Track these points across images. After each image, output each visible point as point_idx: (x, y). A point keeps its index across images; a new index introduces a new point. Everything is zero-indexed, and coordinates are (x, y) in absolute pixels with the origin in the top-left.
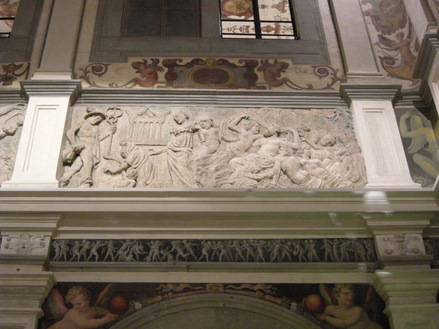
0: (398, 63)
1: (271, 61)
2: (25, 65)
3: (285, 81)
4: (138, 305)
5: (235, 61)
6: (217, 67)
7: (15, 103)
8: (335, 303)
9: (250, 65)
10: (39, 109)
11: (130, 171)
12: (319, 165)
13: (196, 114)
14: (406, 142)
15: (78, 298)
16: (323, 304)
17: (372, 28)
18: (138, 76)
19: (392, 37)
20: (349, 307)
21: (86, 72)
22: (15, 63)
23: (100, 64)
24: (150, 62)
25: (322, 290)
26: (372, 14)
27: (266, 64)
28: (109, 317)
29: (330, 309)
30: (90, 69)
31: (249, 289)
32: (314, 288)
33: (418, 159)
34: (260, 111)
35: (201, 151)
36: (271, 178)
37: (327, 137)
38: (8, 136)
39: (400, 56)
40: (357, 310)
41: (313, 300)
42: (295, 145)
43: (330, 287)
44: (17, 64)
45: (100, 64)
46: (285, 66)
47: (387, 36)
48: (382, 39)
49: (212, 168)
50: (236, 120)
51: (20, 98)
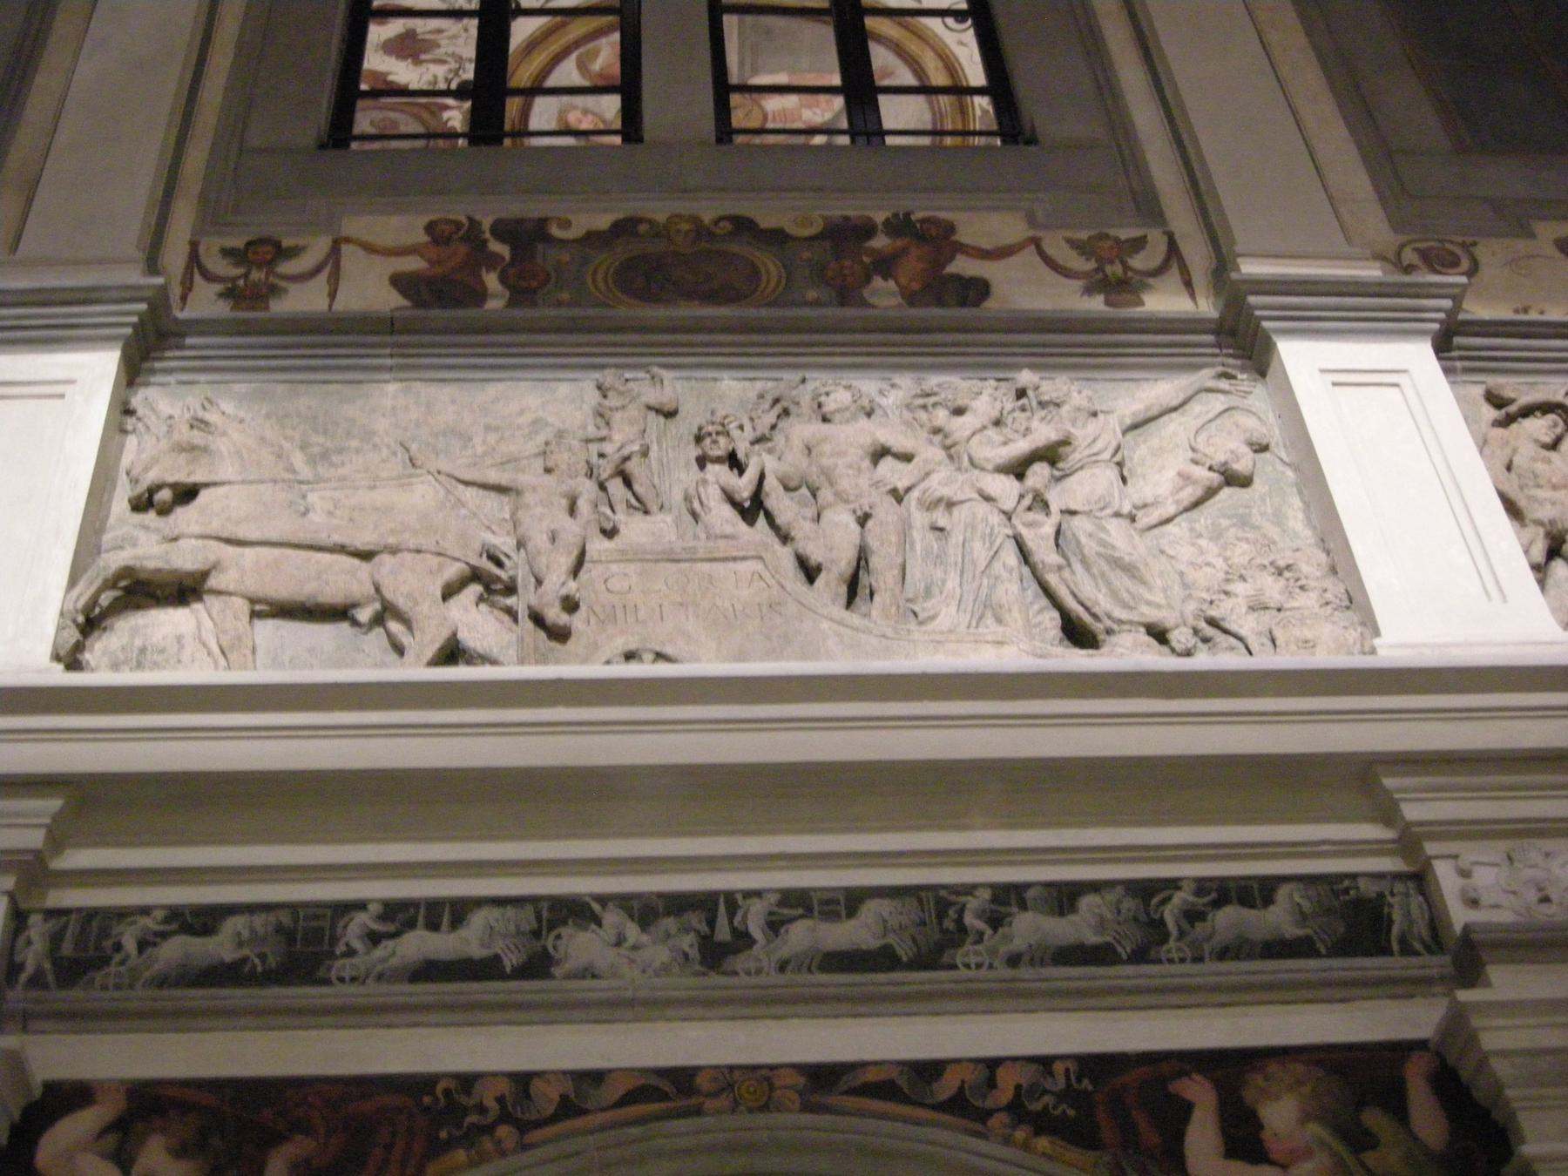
7: (1199, 367)
10: (1334, 384)
22: (1113, 232)
23: (1441, 241)
38: (1226, 492)
44: (1124, 234)
45: (1441, 241)
51: (1217, 351)
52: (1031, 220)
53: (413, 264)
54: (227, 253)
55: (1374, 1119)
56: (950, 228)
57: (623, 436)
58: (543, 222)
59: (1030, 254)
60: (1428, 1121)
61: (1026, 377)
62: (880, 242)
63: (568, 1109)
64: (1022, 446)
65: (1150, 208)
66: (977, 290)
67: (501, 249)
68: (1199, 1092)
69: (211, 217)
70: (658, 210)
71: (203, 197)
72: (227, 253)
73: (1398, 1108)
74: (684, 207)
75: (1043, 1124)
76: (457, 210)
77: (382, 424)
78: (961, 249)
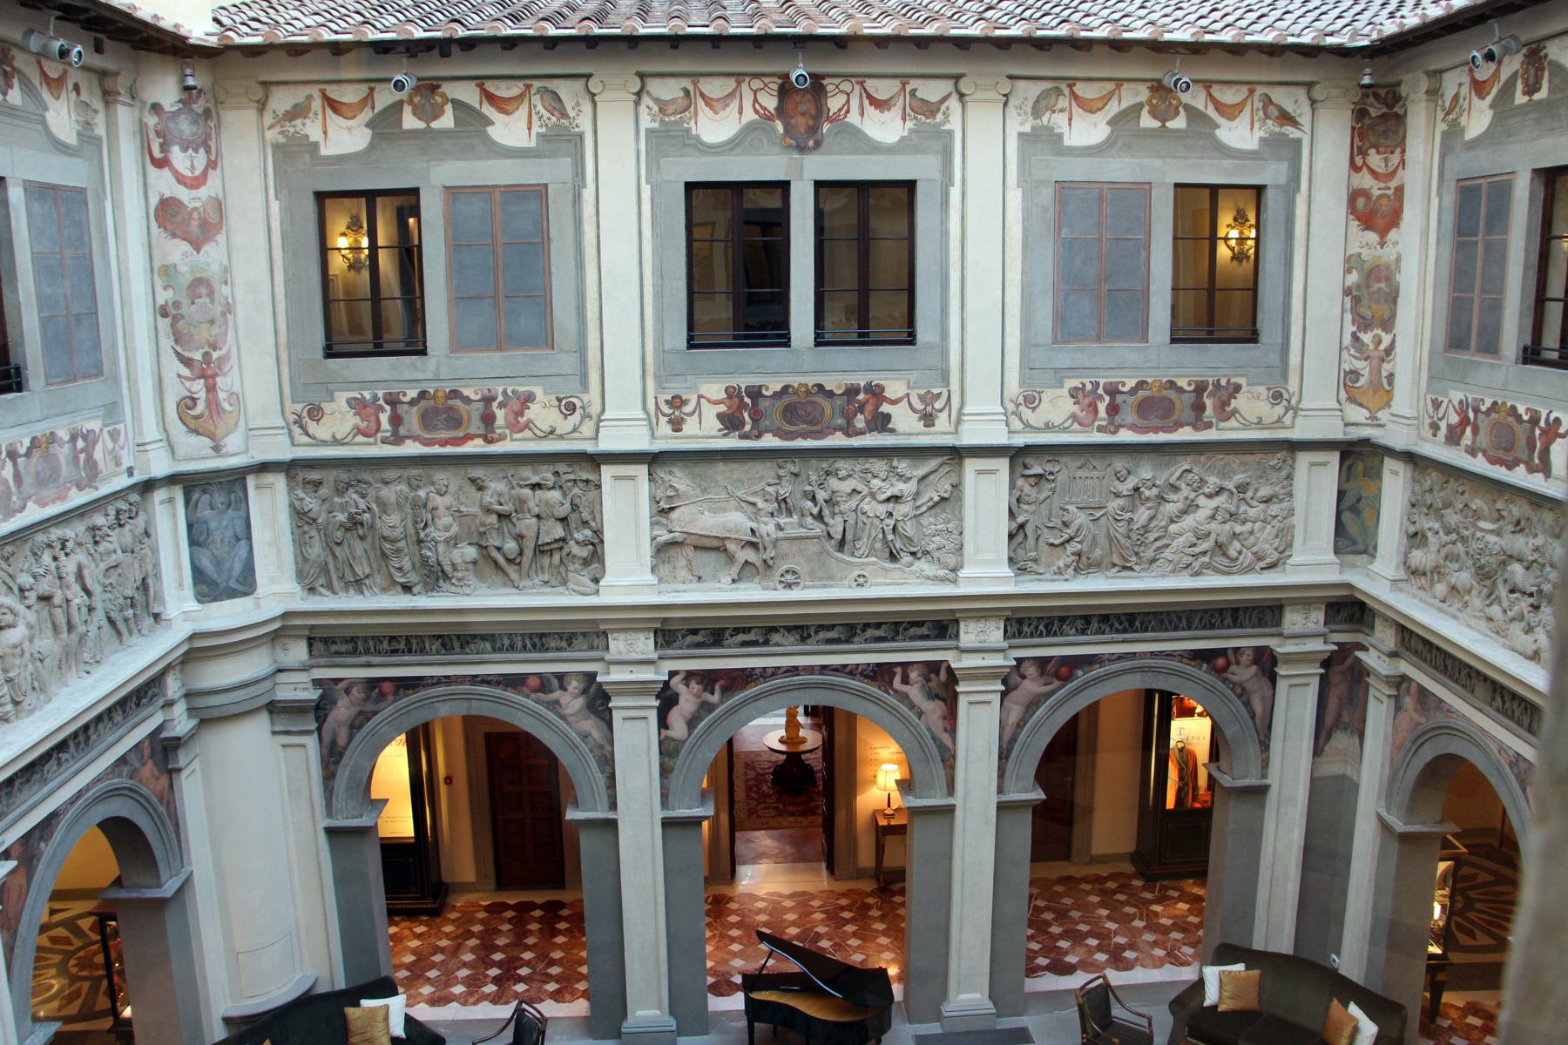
0: (1362, 381)
1: (1223, 382)
2: (945, 394)
3: (1235, 411)
4: (1080, 673)
5: (1182, 383)
6: (1165, 393)
8: (1238, 663)
9: (1200, 388)
11: (1073, 547)
12: (1251, 533)
13: (1137, 465)
14: (1341, 495)
15: (1031, 670)
16: (1228, 664)
17: (1348, 317)
18: (1076, 409)
19: (1366, 338)
20: (1248, 666)
21: (1018, 405)
24: (1089, 387)
25: (1230, 653)
26: (1355, 293)
27: (1217, 385)
28: (1057, 683)
29: (1233, 668)
30: (1021, 400)
31: (1169, 655)
32: (1222, 652)
33: (1346, 516)
34: (1202, 459)
35: (1142, 515)
36: (1205, 553)
37: (1265, 491)
39: (1366, 372)
40: (1254, 669)
41: (1221, 662)
42: (1233, 509)
43: (1236, 650)
44: (935, 391)
46: (1238, 388)
47: (1361, 335)
48: (1355, 337)
49: (1151, 536)
50: (1177, 474)
52: (909, 387)
53: (722, 408)
54: (667, 402)
55: (932, 676)
56: (882, 388)
57: (785, 490)
58: (760, 387)
59: (905, 403)
60: (943, 676)
61: (895, 463)
62: (861, 397)
63: (773, 674)
64: (888, 494)
65: (945, 379)
66: (887, 418)
67: (747, 400)
68: (898, 670)
69: (660, 387)
70: (795, 381)
71: (655, 377)
72: (667, 402)
73: (938, 673)
74: (803, 380)
75: (866, 677)
76: (734, 381)
77: (720, 478)
78: (885, 399)
